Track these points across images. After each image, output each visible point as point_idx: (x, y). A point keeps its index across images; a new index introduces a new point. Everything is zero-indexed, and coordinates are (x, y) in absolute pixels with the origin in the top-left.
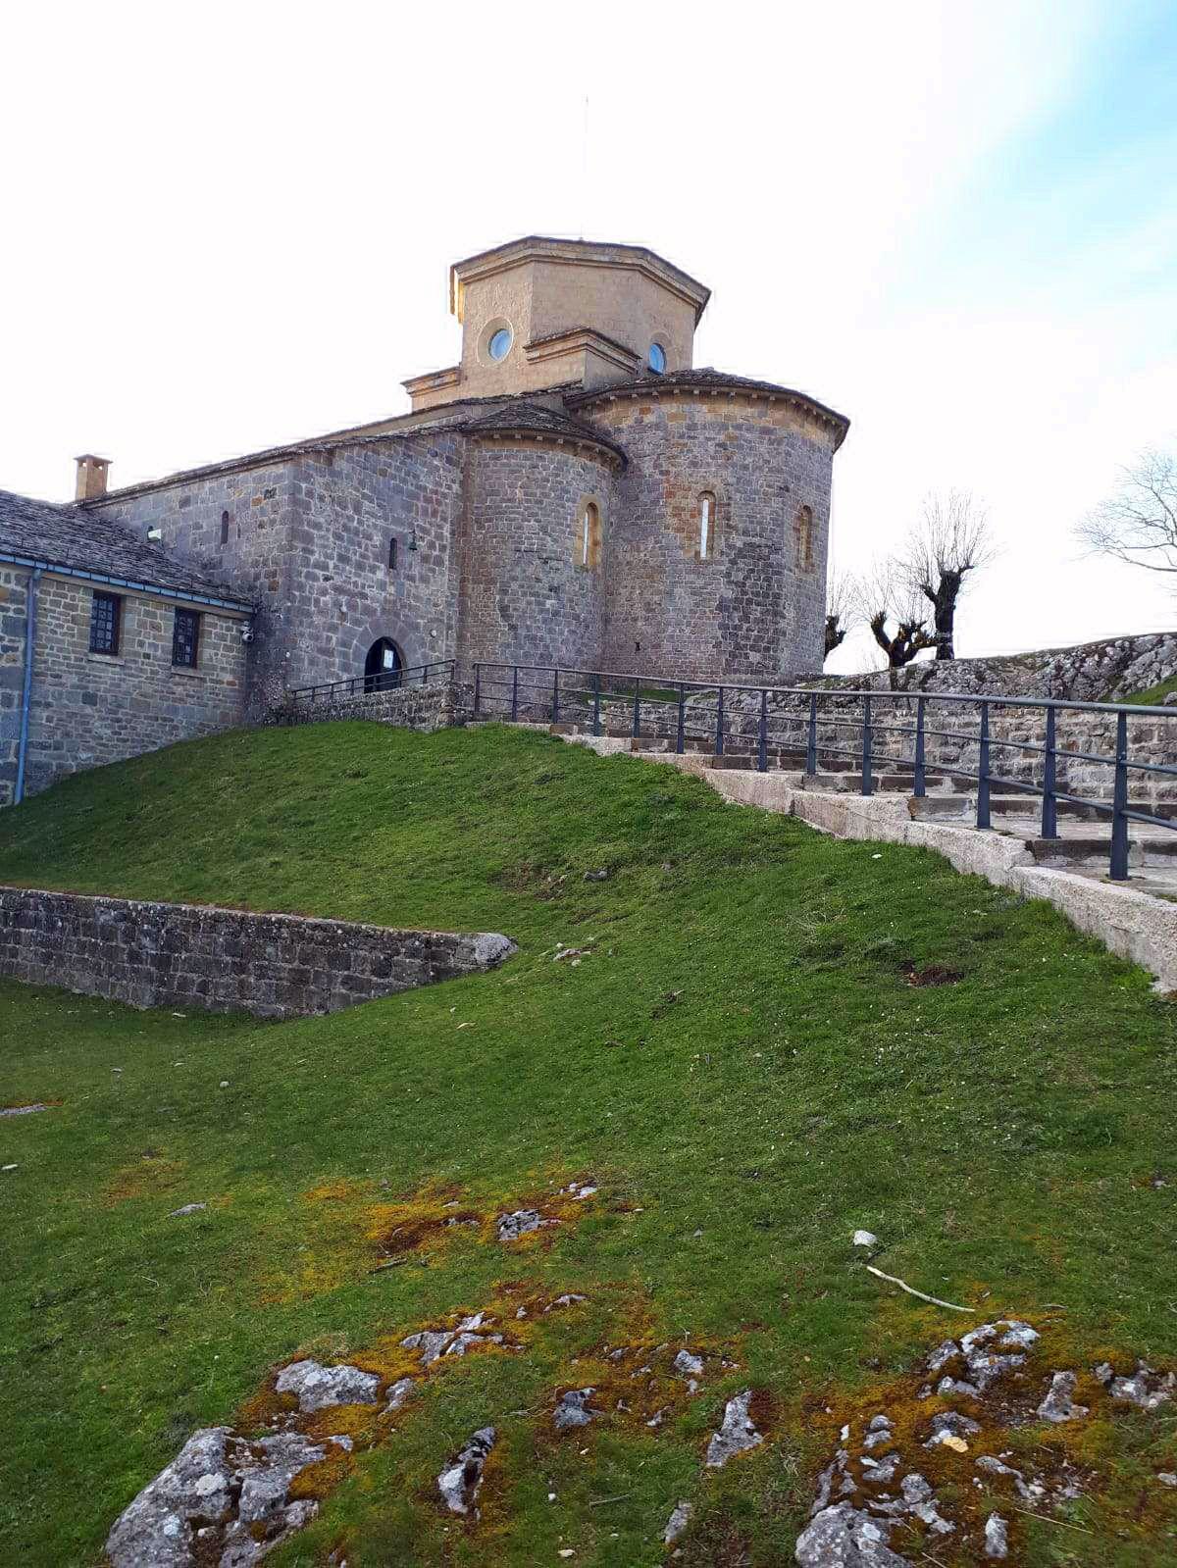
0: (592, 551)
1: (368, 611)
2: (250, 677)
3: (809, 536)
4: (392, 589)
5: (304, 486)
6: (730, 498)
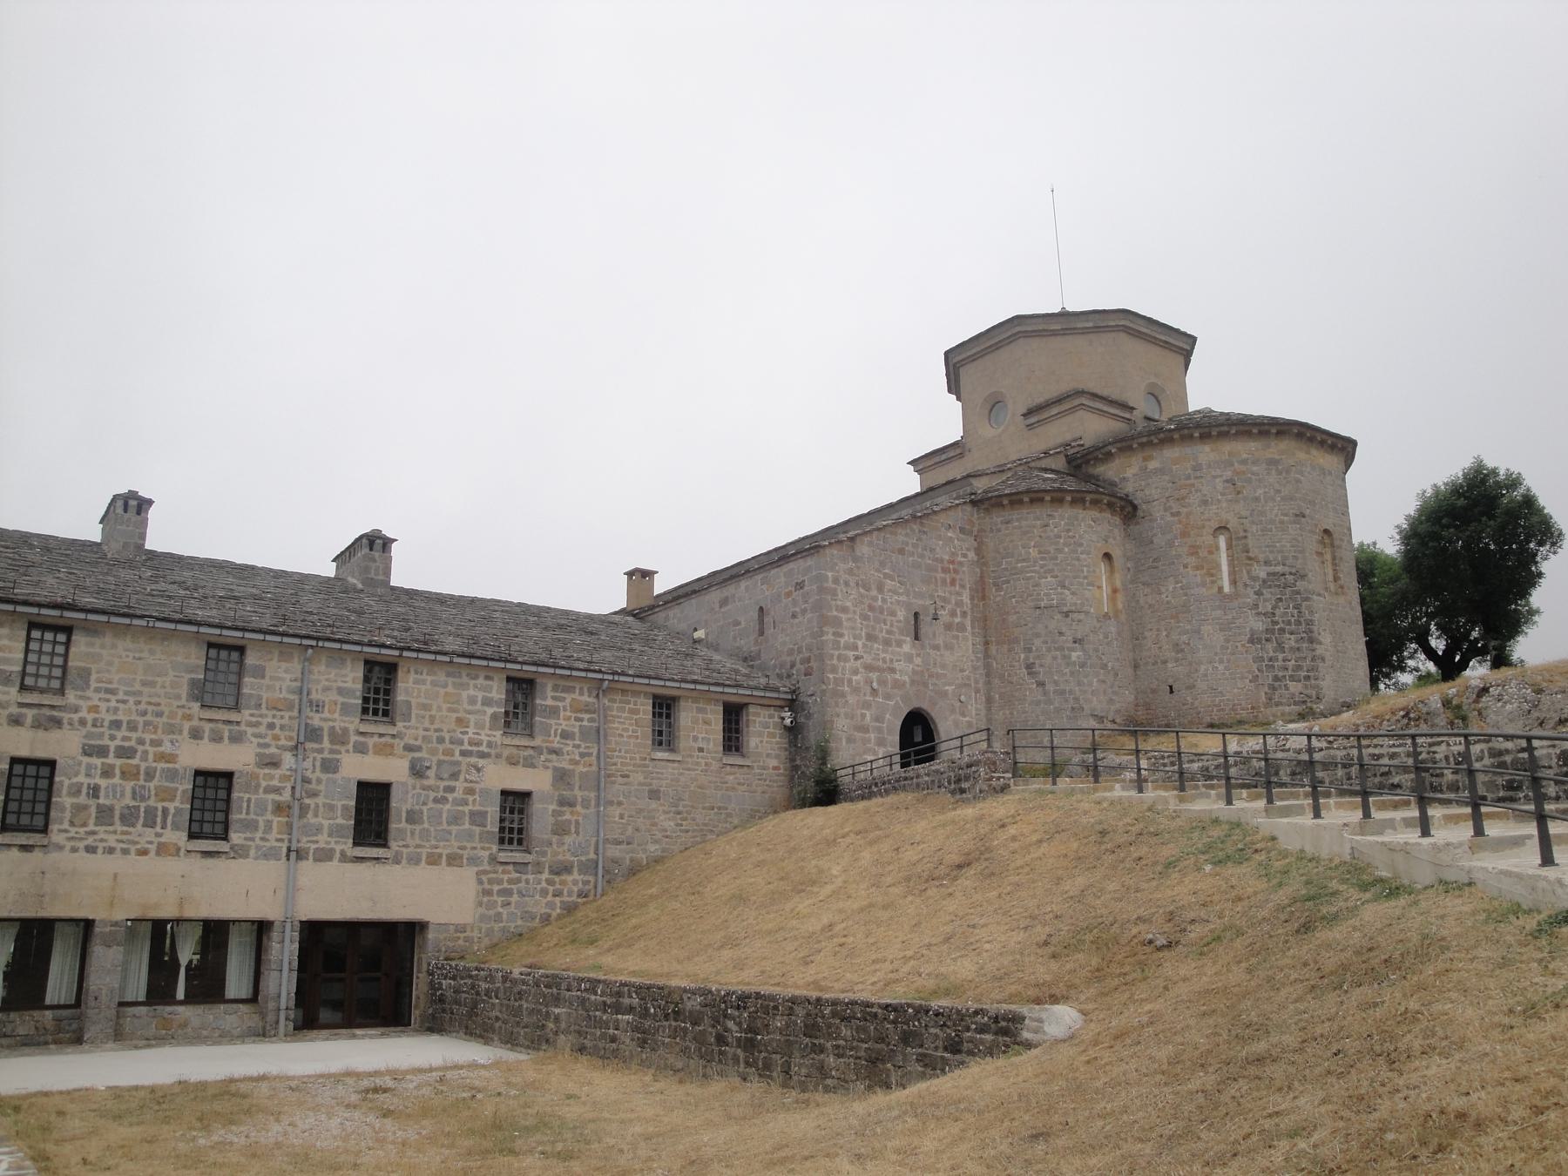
0: (1112, 599)
1: (898, 685)
2: (792, 760)
3: (1334, 558)
4: (918, 661)
5: (830, 574)
6: (1245, 531)
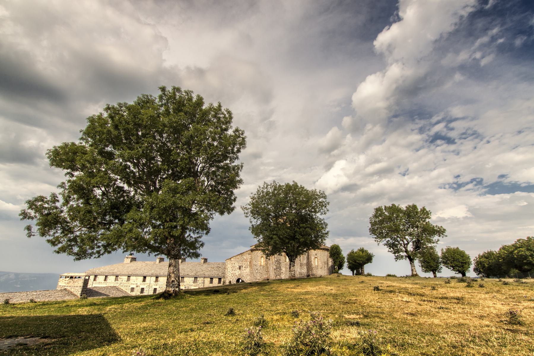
1: (236, 275)
